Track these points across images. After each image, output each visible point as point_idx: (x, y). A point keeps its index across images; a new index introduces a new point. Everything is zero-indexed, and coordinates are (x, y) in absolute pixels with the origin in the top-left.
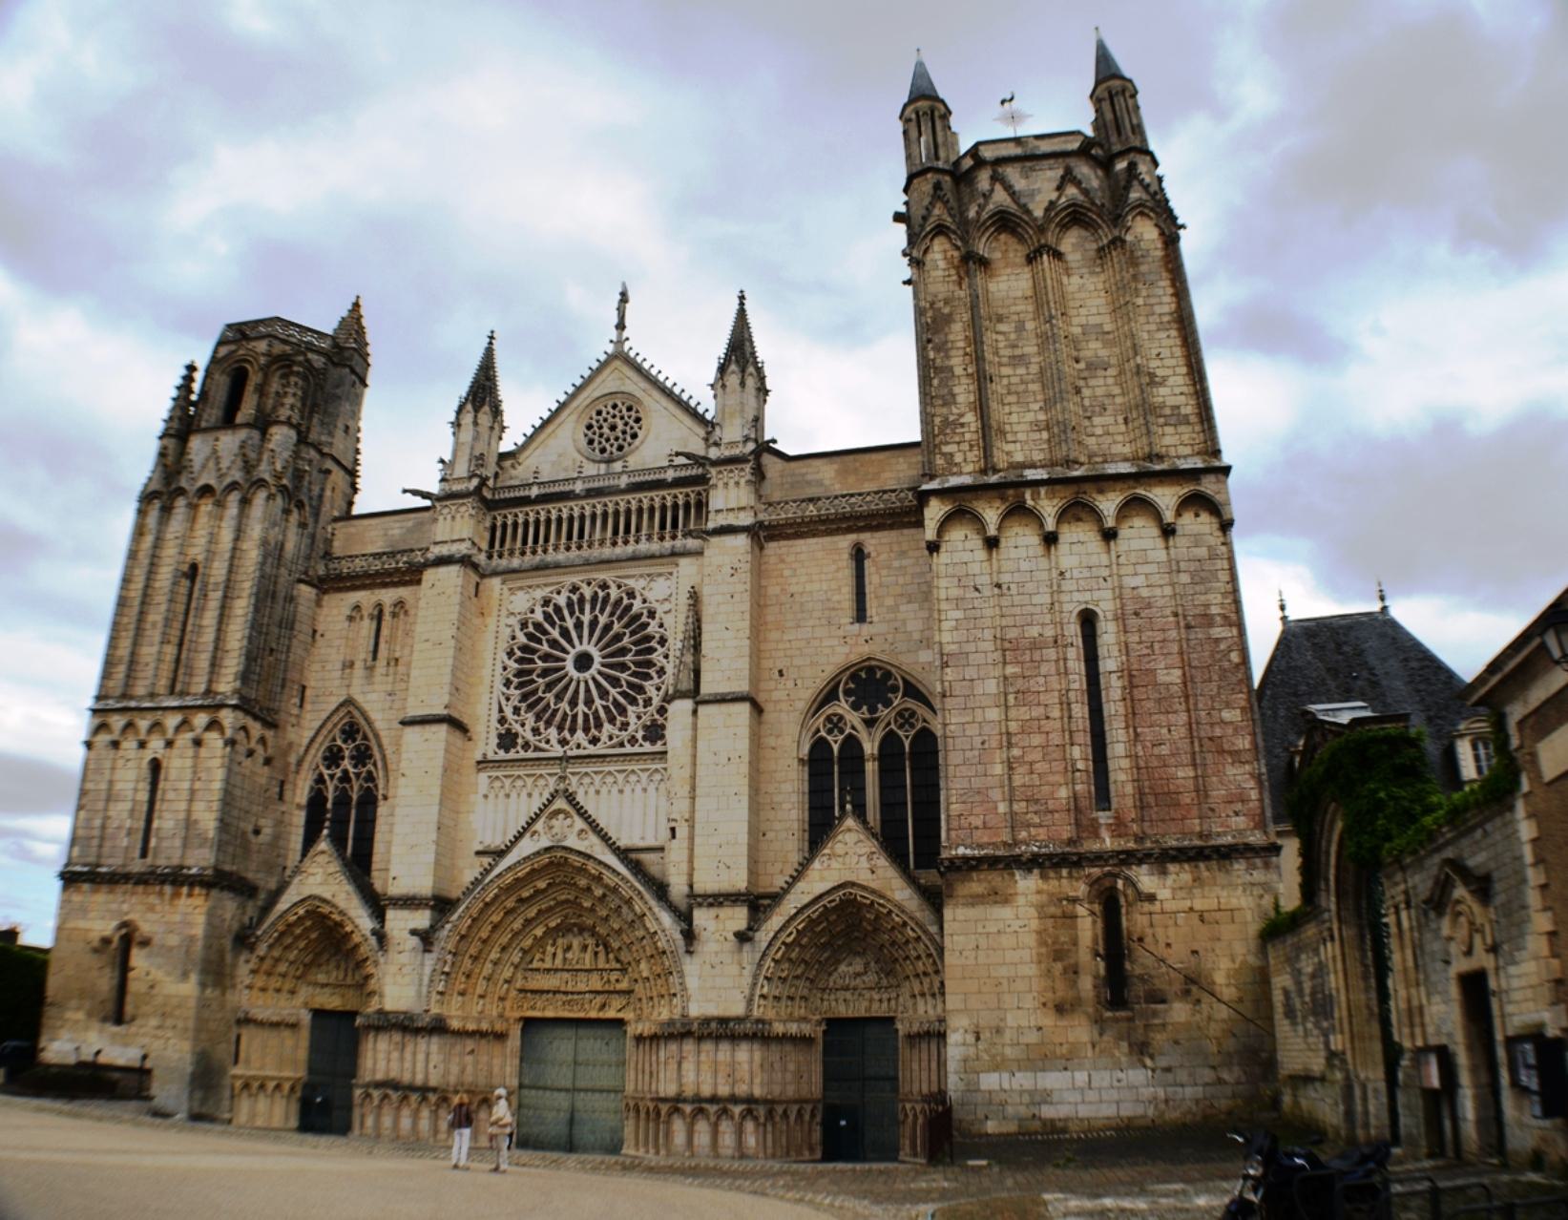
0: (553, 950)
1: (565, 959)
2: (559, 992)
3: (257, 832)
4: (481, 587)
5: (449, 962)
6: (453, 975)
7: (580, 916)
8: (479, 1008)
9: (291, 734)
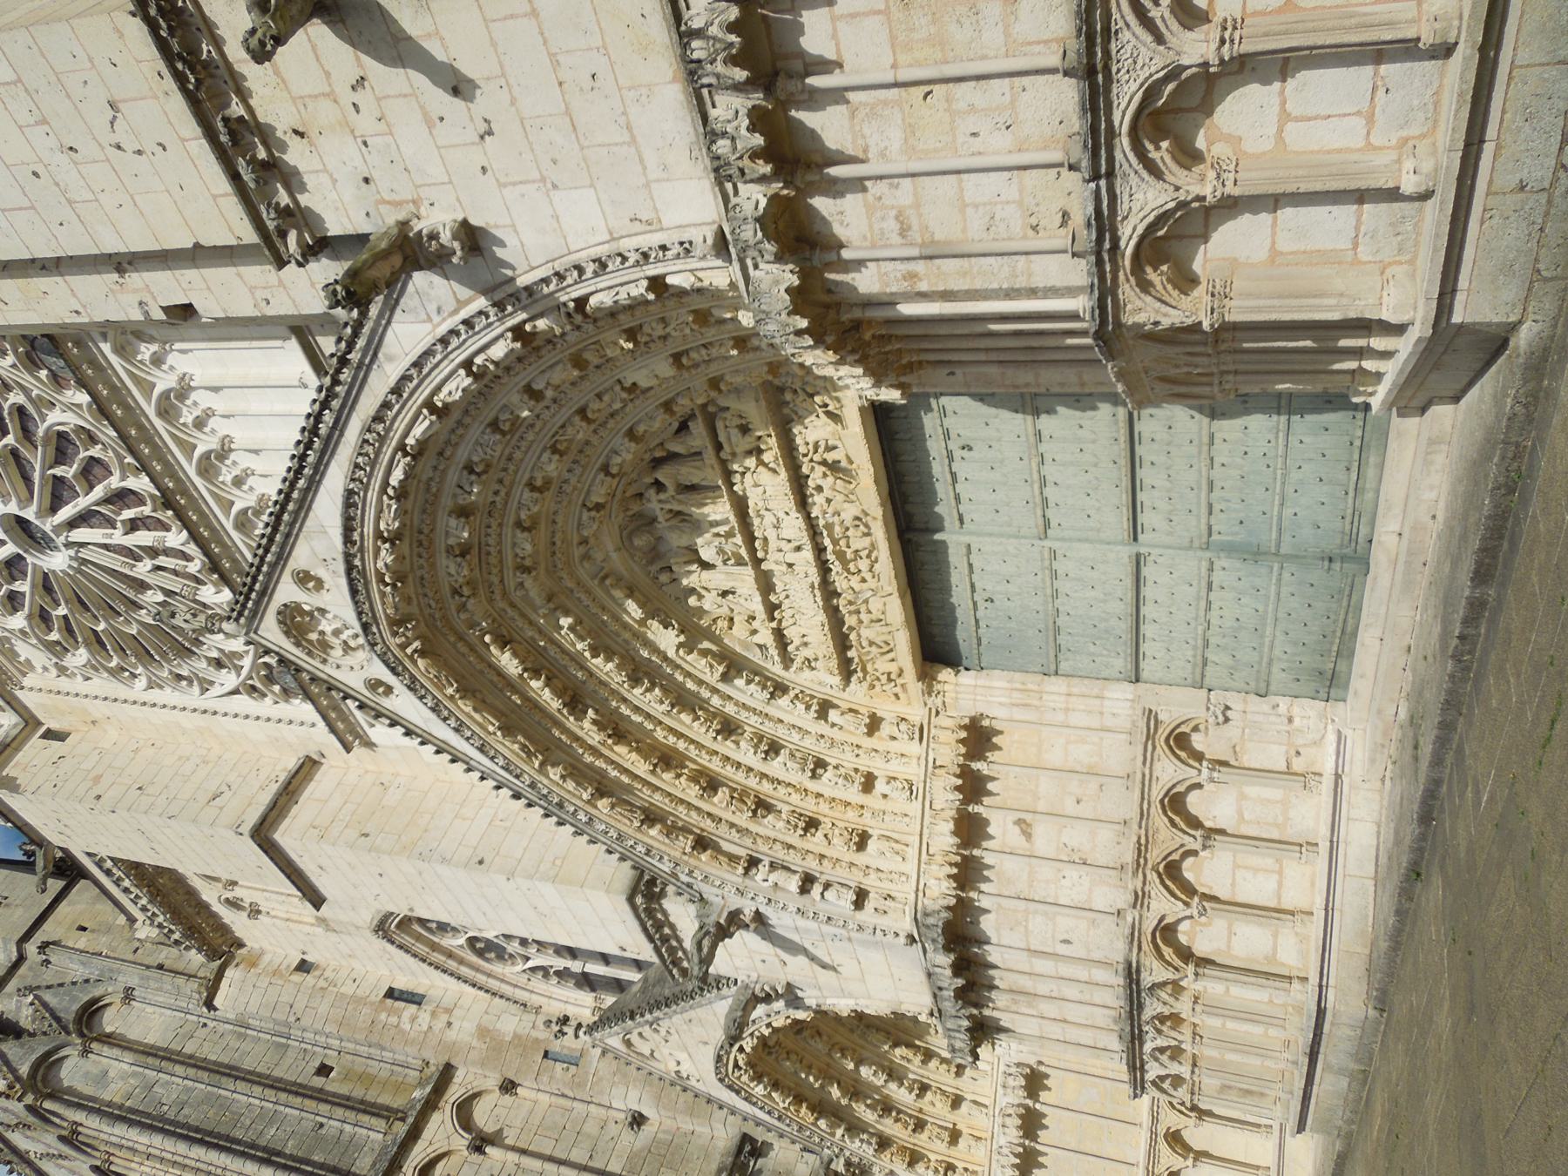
3: (638, 1120)
4: (54, 725)
5: (773, 877)
6: (812, 865)
9: (463, 1031)
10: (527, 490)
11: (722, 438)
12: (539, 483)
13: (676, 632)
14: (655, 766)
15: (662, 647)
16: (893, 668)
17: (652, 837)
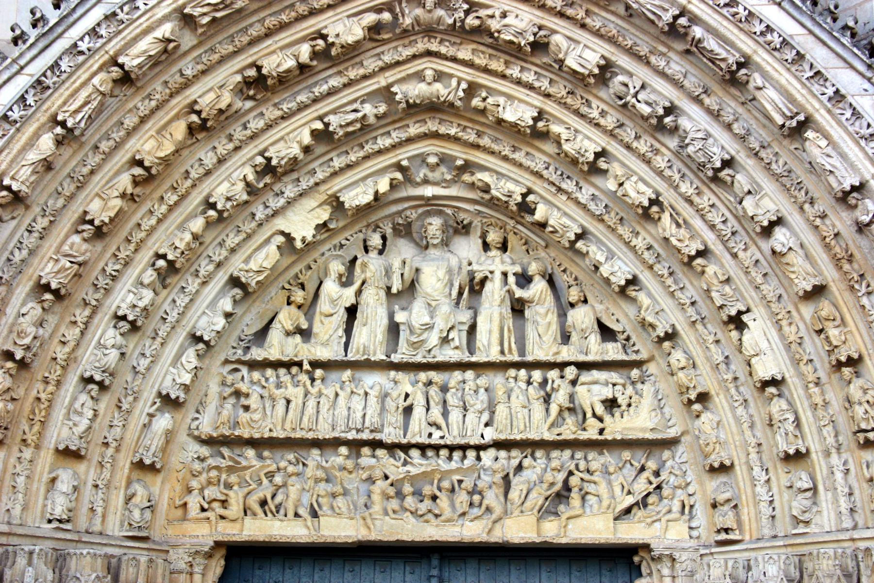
0: (348, 296)
1: (394, 329)
2: (376, 444)
7: (468, 167)
8: (59, 507)
10: (599, 149)
11: (596, 374)
12: (602, 164)
13: (309, 238)
14: (148, 169)
15: (290, 214)
16: (235, 509)
17: (37, 135)
